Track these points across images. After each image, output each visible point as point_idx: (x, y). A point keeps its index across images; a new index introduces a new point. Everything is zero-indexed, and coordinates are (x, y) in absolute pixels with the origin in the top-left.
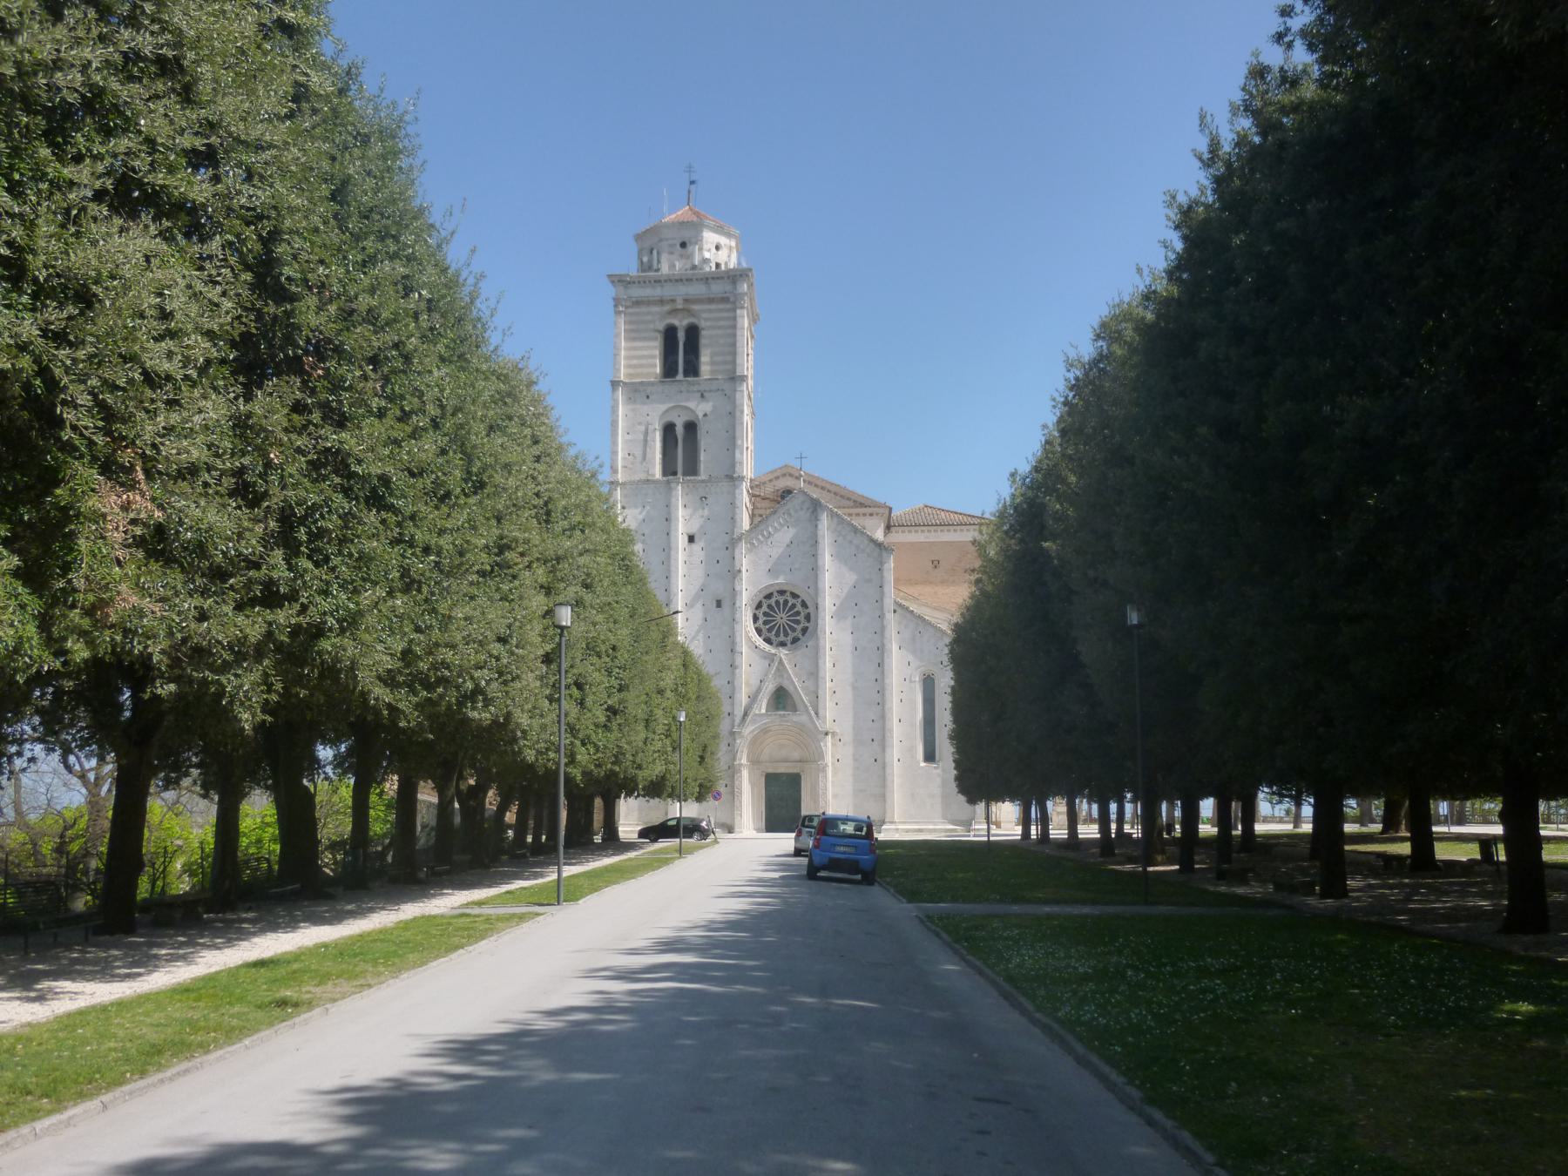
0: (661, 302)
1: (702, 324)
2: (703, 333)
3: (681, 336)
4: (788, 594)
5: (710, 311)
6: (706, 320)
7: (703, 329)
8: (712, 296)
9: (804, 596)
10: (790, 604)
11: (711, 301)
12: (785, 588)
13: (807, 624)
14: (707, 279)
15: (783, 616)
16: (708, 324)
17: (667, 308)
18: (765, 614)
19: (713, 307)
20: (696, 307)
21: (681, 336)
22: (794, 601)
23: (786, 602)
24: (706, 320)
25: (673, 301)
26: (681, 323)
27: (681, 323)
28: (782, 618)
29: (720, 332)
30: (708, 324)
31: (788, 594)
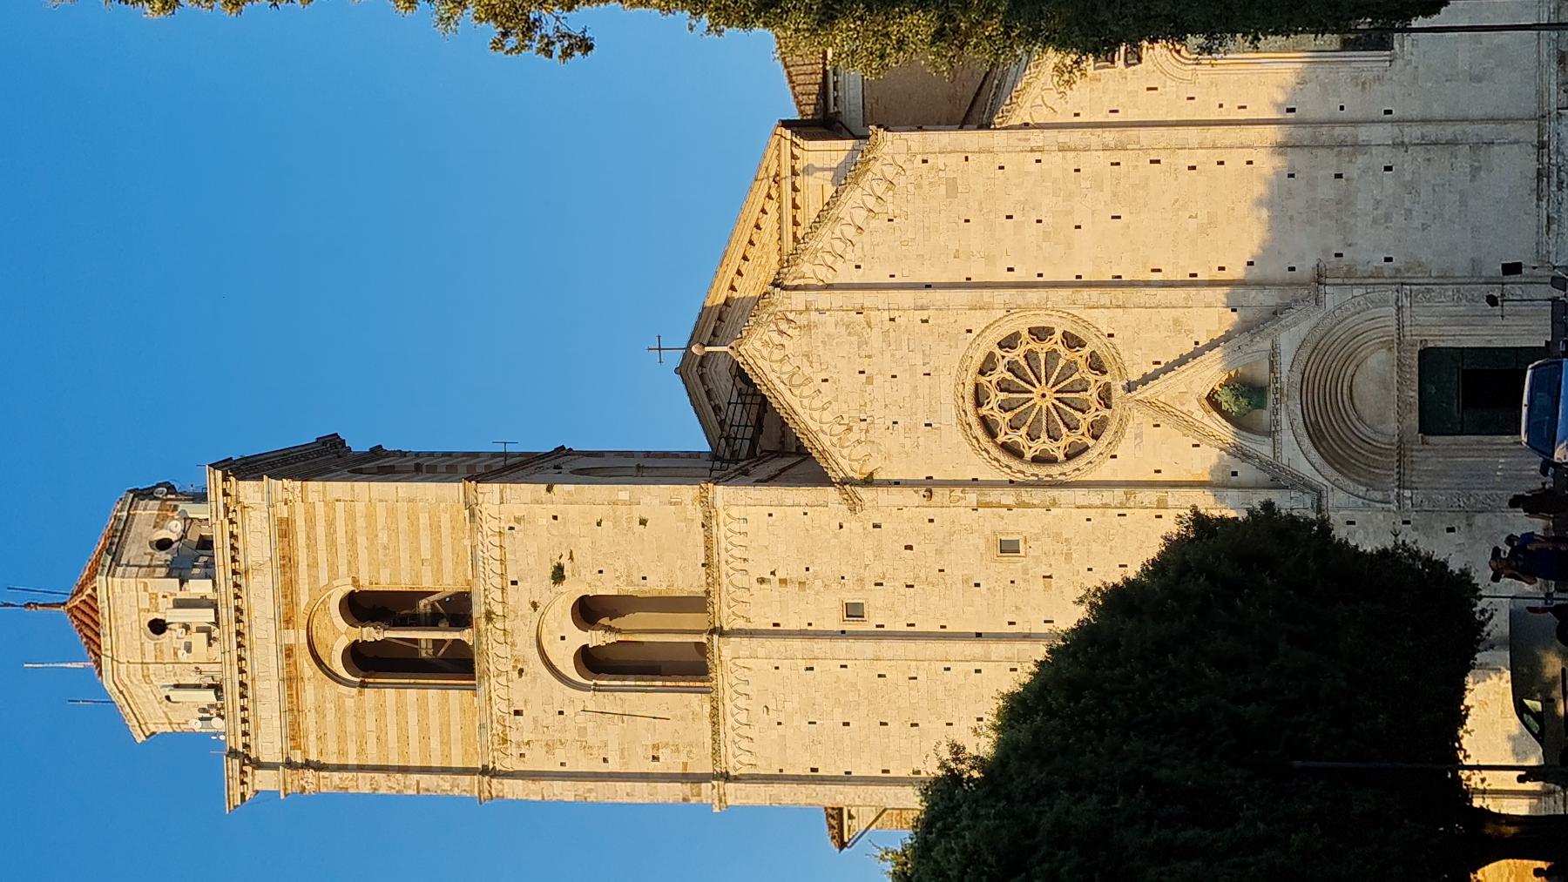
0: (291, 681)
1: (344, 588)
2: (365, 585)
3: (370, 634)
4: (983, 380)
5: (313, 565)
6: (334, 574)
7: (355, 581)
8: (277, 562)
9: (989, 343)
10: (1009, 376)
11: (287, 563)
12: (969, 390)
13: (1058, 336)
14: (234, 572)
15: (1037, 391)
16: (343, 569)
17: (307, 667)
18: (1032, 437)
19: (302, 557)
20: (304, 599)
21: (370, 634)
22: (1001, 367)
23: (1003, 386)
24: (334, 574)
25: (289, 652)
26: (339, 635)
27: (339, 635)
28: (1042, 397)
29: (362, 541)
30: (343, 569)
31: (983, 380)
